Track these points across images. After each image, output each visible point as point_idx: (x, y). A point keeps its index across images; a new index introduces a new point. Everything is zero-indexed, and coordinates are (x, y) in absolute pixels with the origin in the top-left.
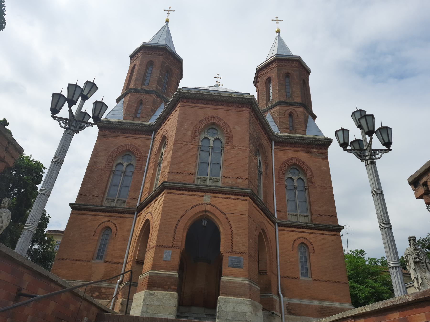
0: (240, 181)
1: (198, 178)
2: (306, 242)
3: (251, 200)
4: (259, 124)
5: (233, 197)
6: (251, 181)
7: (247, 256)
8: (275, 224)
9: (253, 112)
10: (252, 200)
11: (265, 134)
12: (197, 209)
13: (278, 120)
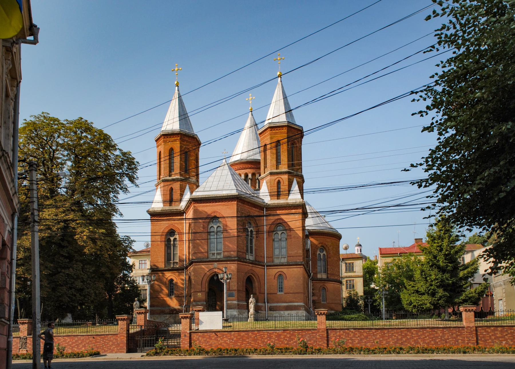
0: (232, 253)
1: (210, 253)
2: (282, 273)
3: (239, 262)
4: (248, 205)
5: (228, 262)
6: (240, 250)
7: (236, 291)
8: (264, 266)
9: (240, 202)
10: (240, 262)
11: (256, 208)
12: (211, 272)
13: (269, 188)
